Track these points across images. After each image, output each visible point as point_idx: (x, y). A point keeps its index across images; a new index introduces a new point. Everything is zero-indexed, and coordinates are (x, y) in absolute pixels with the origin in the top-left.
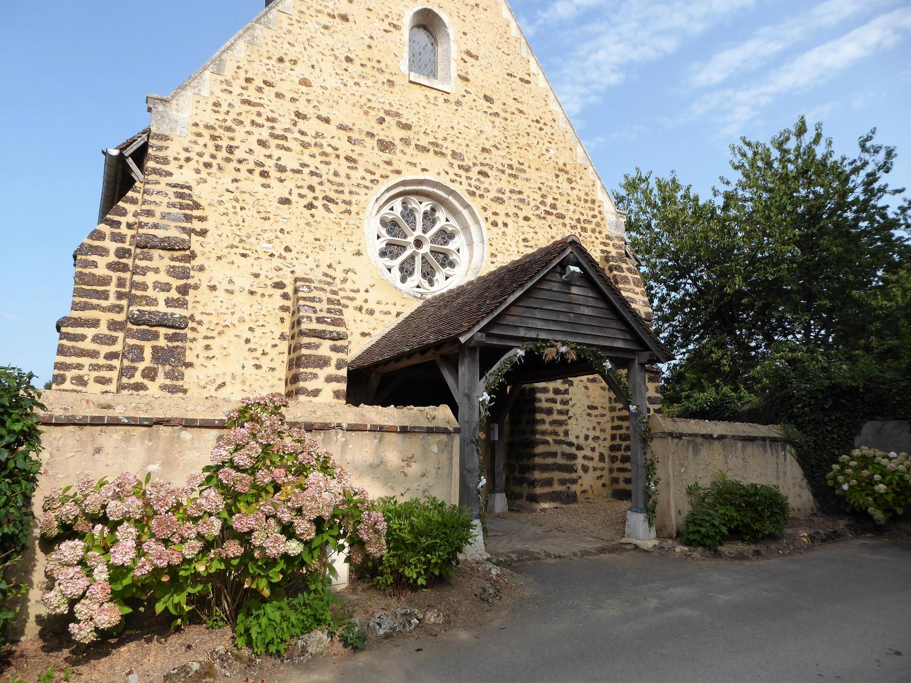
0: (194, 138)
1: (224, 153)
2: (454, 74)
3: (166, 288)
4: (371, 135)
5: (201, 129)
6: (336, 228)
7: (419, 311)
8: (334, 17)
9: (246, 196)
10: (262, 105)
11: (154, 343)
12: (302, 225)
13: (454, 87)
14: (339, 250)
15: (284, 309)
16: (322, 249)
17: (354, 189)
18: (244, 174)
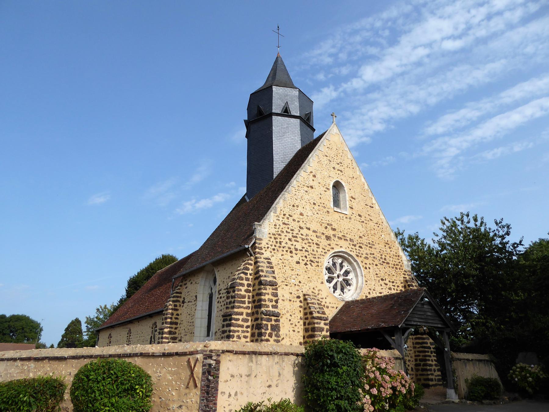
0: (269, 239)
1: (278, 245)
2: (348, 207)
3: (271, 301)
4: (323, 234)
5: (271, 236)
6: (314, 273)
7: (344, 306)
8: (308, 187)
9: (286, 261)
10: (289, 224)
11: (271, 323)
12: (304, 272)
13: (348, 212)
14: (316, 282)
15: (301, 307)
16: (311, 281)
17: (319, 256)
18: (285, 252)
